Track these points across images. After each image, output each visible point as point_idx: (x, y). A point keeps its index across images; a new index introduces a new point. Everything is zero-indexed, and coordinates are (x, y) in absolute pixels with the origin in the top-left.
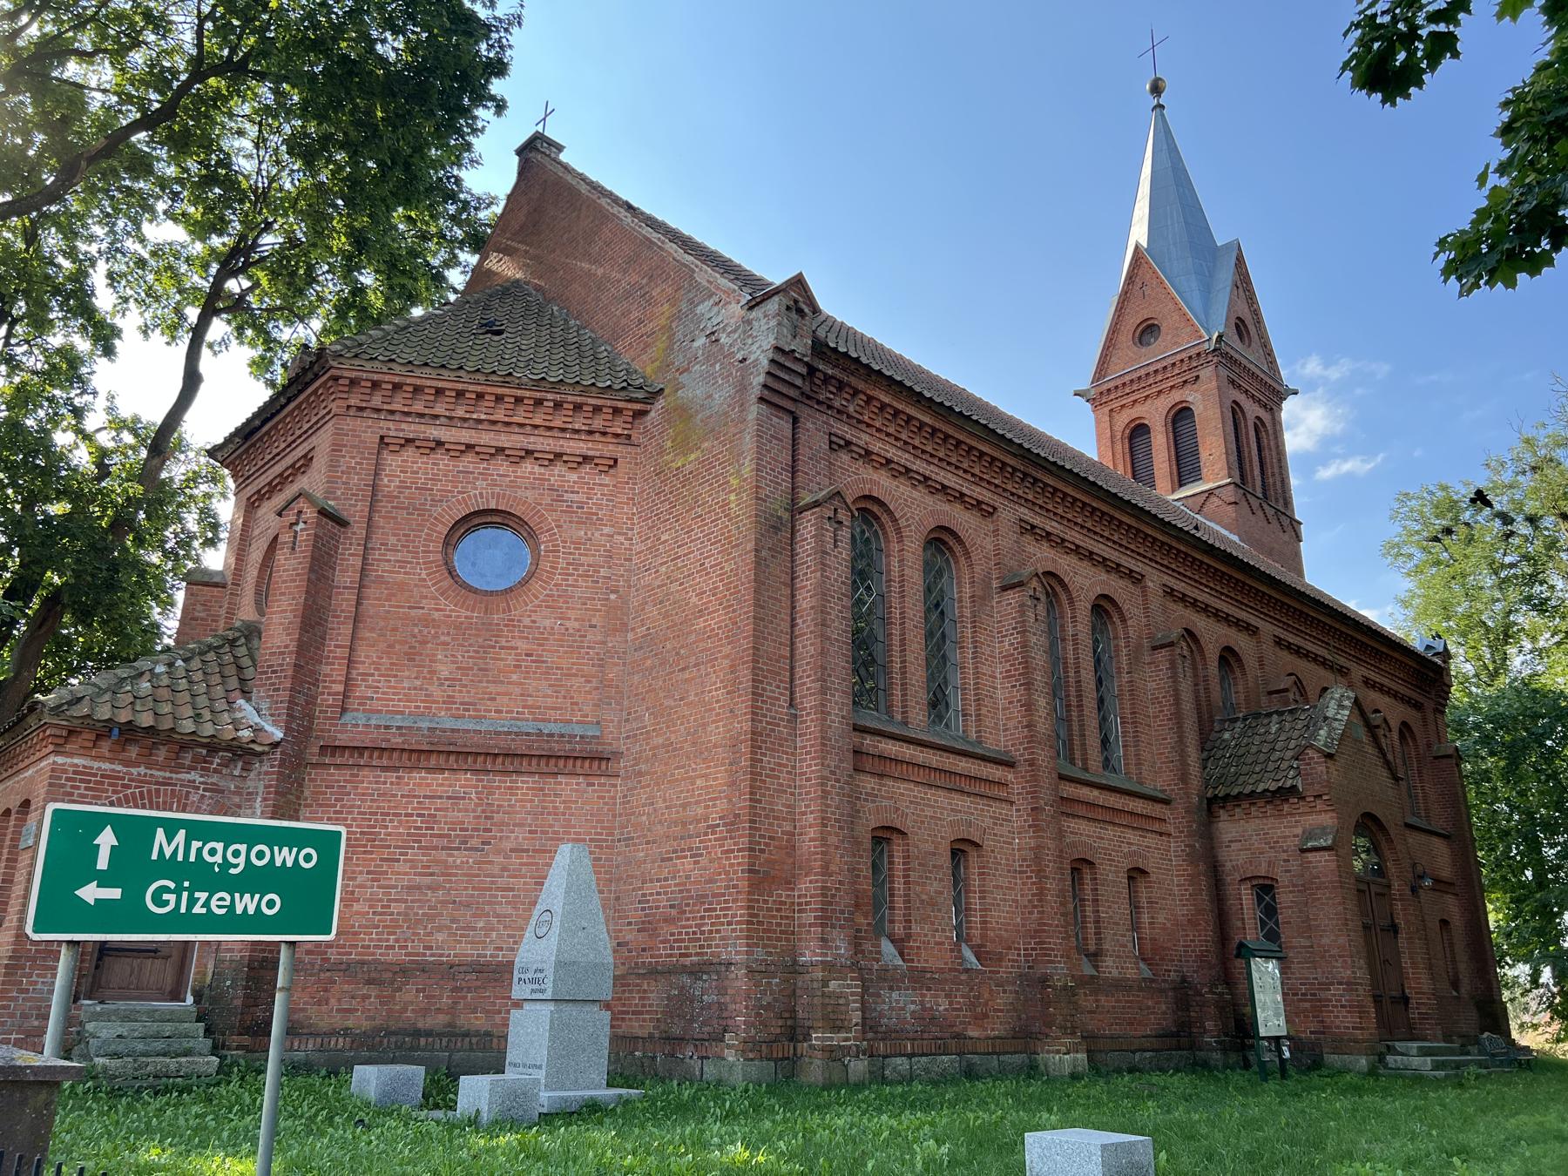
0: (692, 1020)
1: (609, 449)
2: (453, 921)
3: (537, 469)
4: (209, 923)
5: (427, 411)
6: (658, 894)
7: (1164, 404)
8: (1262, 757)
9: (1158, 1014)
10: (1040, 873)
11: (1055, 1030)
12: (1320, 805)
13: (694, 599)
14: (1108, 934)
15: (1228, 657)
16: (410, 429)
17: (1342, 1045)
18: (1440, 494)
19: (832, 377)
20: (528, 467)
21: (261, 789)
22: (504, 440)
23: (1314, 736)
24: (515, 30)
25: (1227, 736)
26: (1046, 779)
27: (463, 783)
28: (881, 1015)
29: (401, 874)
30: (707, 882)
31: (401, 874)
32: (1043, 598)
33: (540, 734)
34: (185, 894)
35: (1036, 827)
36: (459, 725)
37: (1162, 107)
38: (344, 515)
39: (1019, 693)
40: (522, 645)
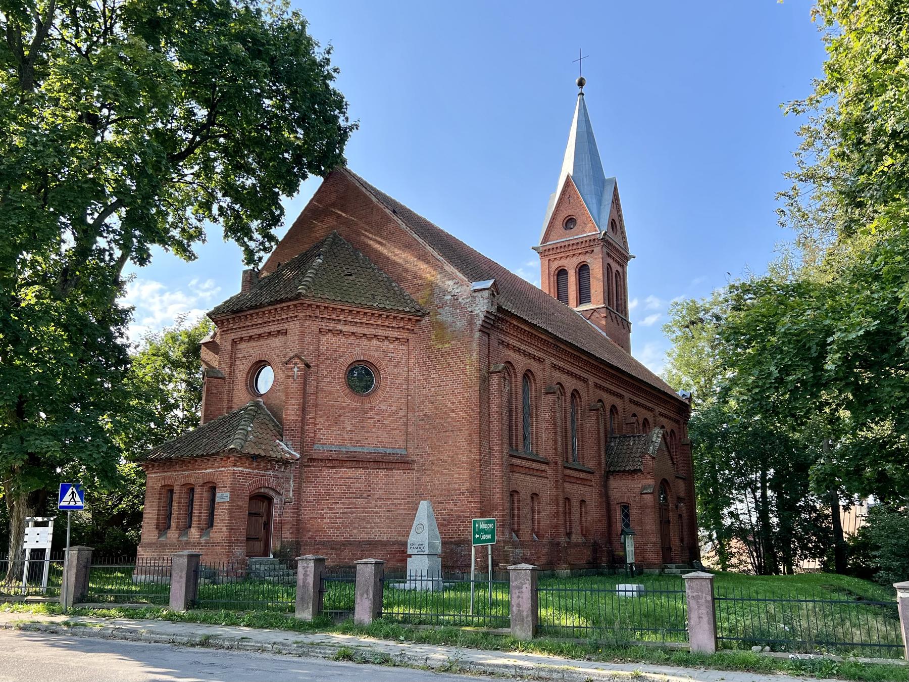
0: (457, 560)
1: (406, 335)
2: (359, 526)
3: (378, 343)
7: (576, 261)
8: (627, 456)
9: (587, 555)
10: (557, 505)
11: (562, 562)
12: (649, 477)
14: (573, 526)
15: (614, 408)
17: (650, 565)
18: (691, 304)
20: (375, 342)
21: (292, 477)
22: (367, 331)
23: (648, 449)
24: (355, 131)
25: (613, 444)
26: (560, 468)
27: (359, 473)
29: (340, 508)
30: (462, 512)
31: (340, 508)
33: (386, 453)
35: (557, 488)
36: (356, 449)
37: (582, 94)
39: (551, 436)
40: (376, 417)
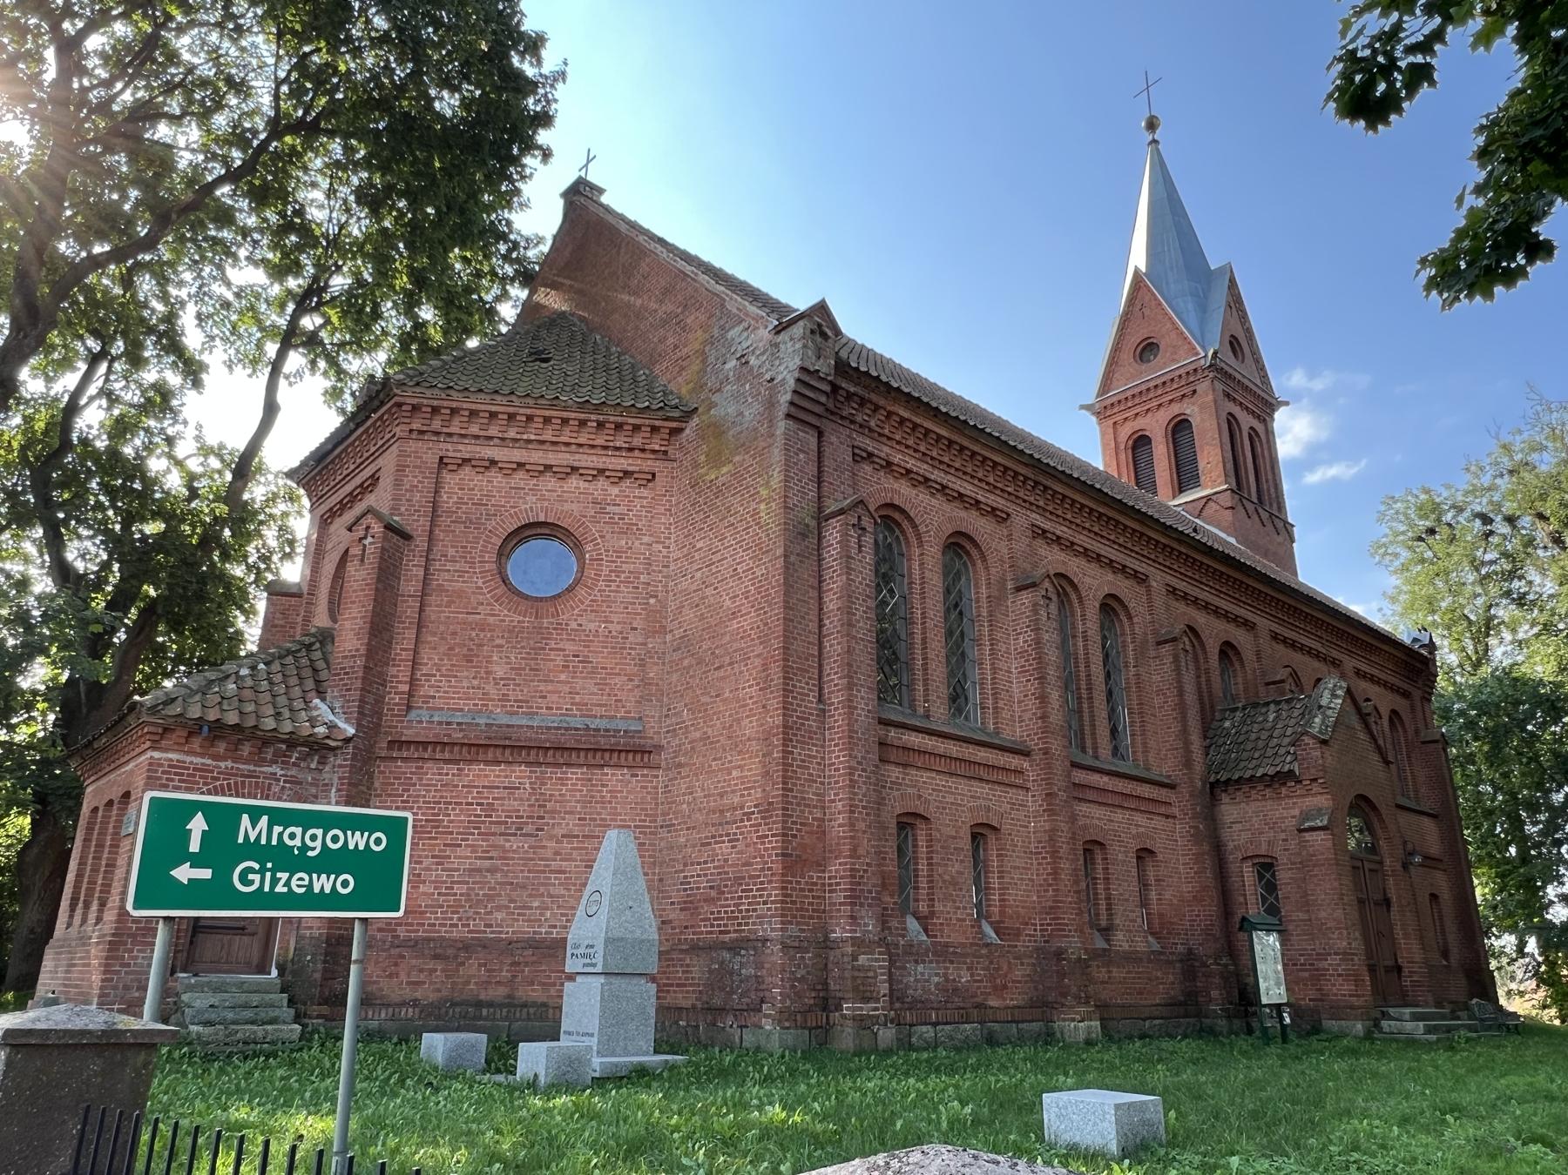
1: (649, 464)
2: (511, 901)
3: (582, 484)
4: (290, 901)
5: (482, 433)
6: (699, 876)
8: (1261, 744)
9: (1166, 984)
10: (1054, 853)
11: (1069, 1000)
12: (1316, 788)
13: (728, 603)
14: (1118, 909)
15: (1228, 651)
16: (467, 450)
17: (1339, 1011)
18: (1423, 497)
19: (854, 394)
20: (574, 482)
21: (336, 781)
22: (552, 458)
23: (1309, 723)
24: (560, 86)
25: (1227, 724)
26: (1059, 767)
27: (519, 774)
28: (907, 986)
29: (463, 858)
30: (744, 865)
31: (463, 858)
32: (1054, 598)
33: (587, 728)
34: (268, 874)
35: (1051, 812)
36: (515, 721)
37: (1154, 141)
38: (408, 529)
39: (1032, 687)
40: (570, 647)
